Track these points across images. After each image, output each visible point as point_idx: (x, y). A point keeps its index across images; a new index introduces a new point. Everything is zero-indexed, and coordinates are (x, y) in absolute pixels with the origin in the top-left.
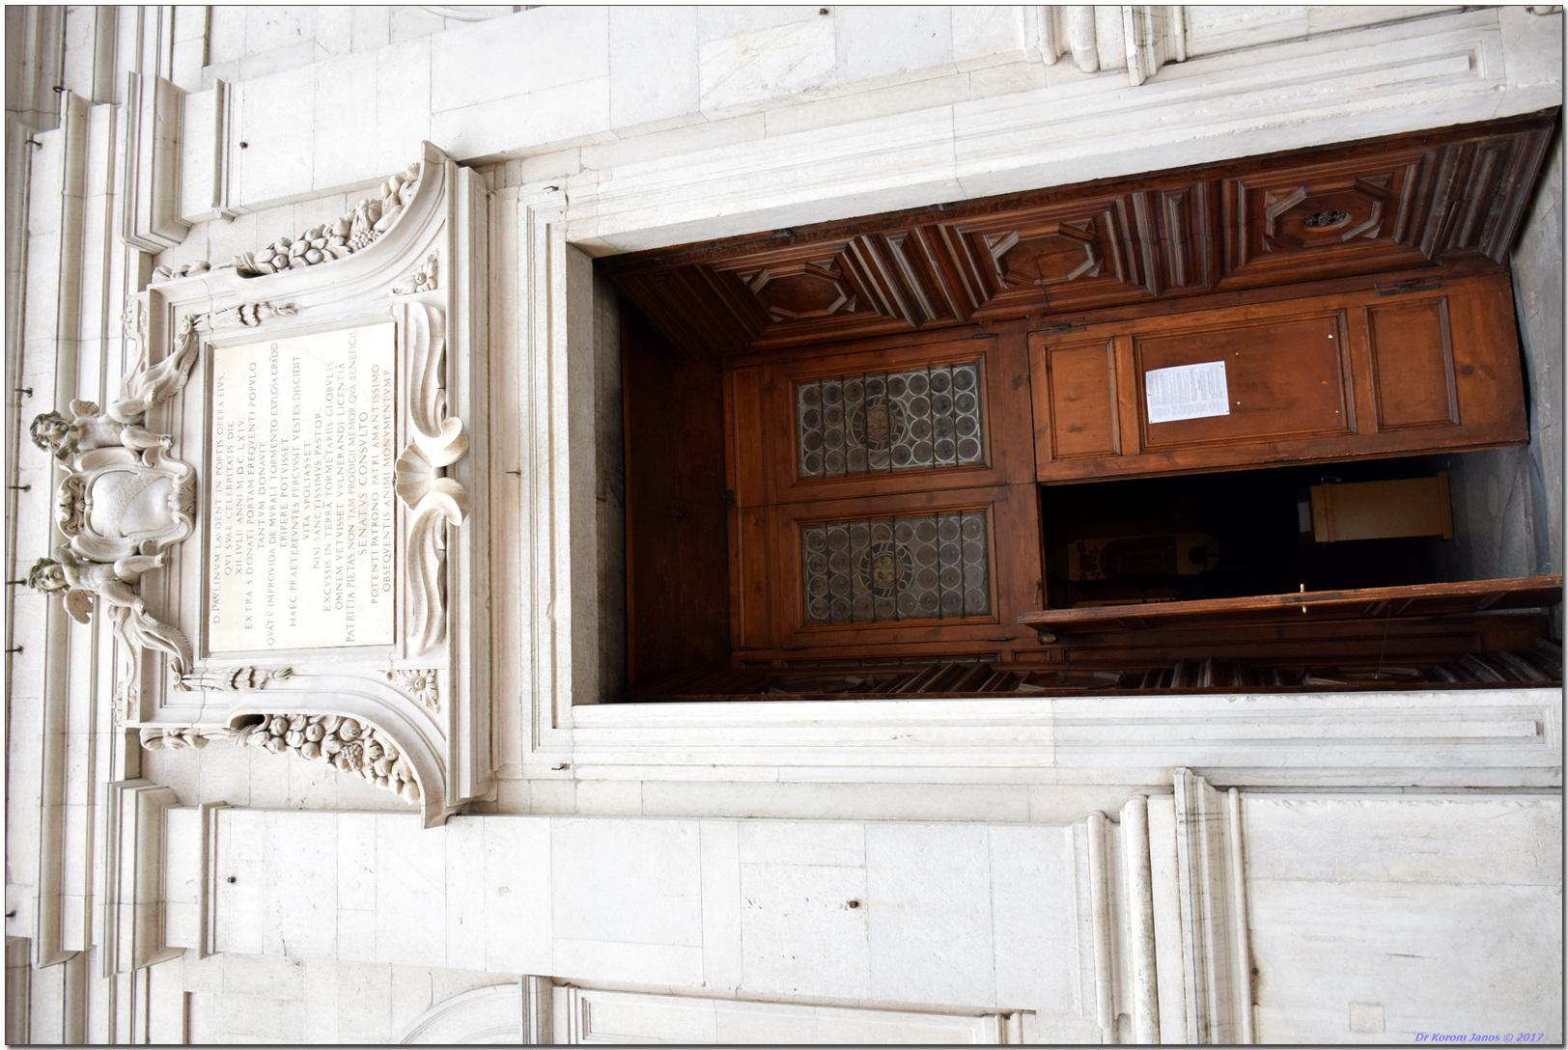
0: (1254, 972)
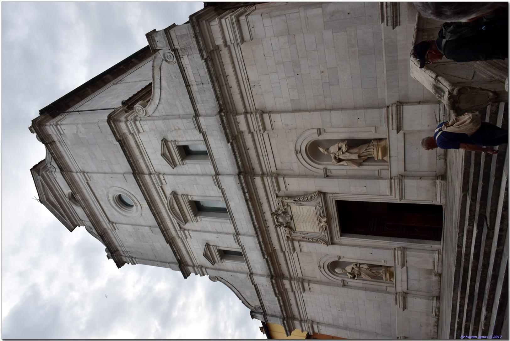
0: (406, 261)
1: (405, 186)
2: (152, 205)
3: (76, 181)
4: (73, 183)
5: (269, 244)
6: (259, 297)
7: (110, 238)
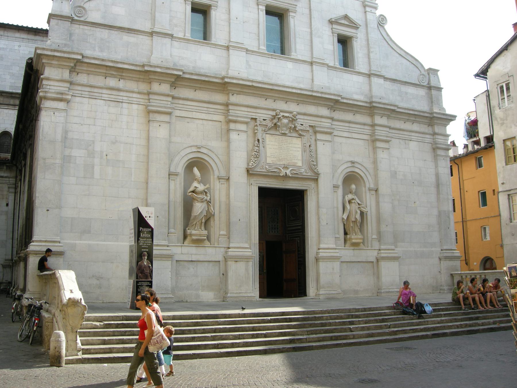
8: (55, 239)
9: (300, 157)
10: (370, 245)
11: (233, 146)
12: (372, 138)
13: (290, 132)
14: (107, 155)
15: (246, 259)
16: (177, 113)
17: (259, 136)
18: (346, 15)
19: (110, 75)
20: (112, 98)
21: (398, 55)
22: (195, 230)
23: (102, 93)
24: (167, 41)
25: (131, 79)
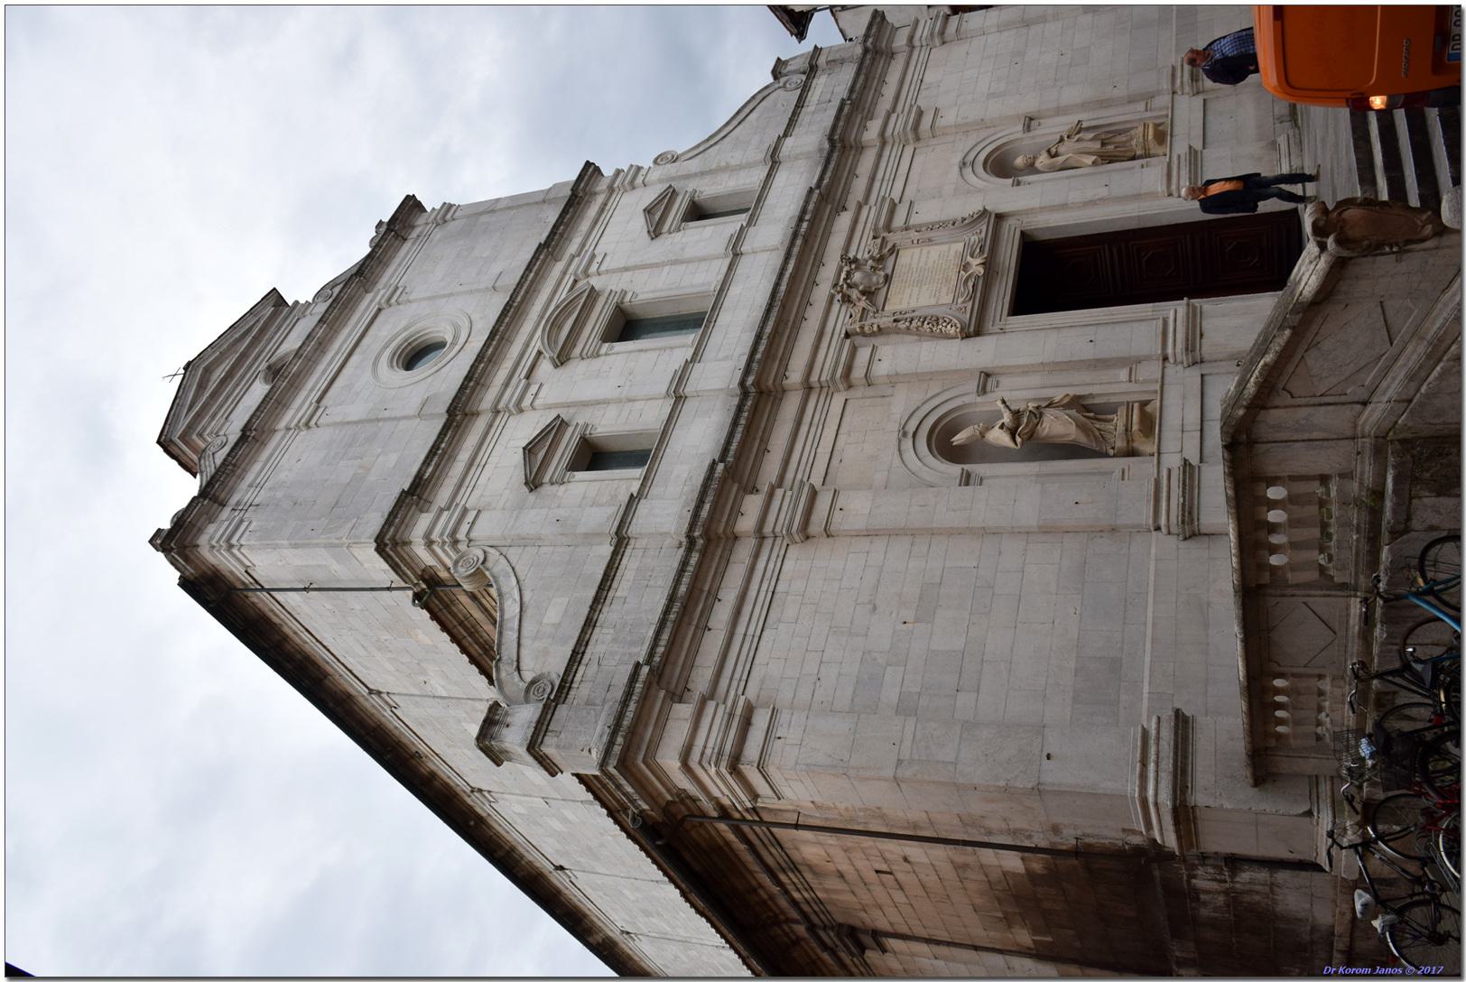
1: (1205, 160)
2: (510, 314)
3: (353, 310)
4: (345, 306)
5: (779, 358)
6: (593, 608)
7: (252, 461)
8: (1136, 740)
9: (945, 247)
10: (1164, 113)
11: (904, 366)
12: (911, 141)
13: (883, 269)
14: (905, 623)
15: (1194, 319)
16: (816, 480)
17: (885, 321)
18: (644, 210)
19: (703, 619)
20: (760, 613)
21: (741, 126)
22: (1116, 429)
23: (745, 635)
24: (643, 508)
25: (720, 575)
